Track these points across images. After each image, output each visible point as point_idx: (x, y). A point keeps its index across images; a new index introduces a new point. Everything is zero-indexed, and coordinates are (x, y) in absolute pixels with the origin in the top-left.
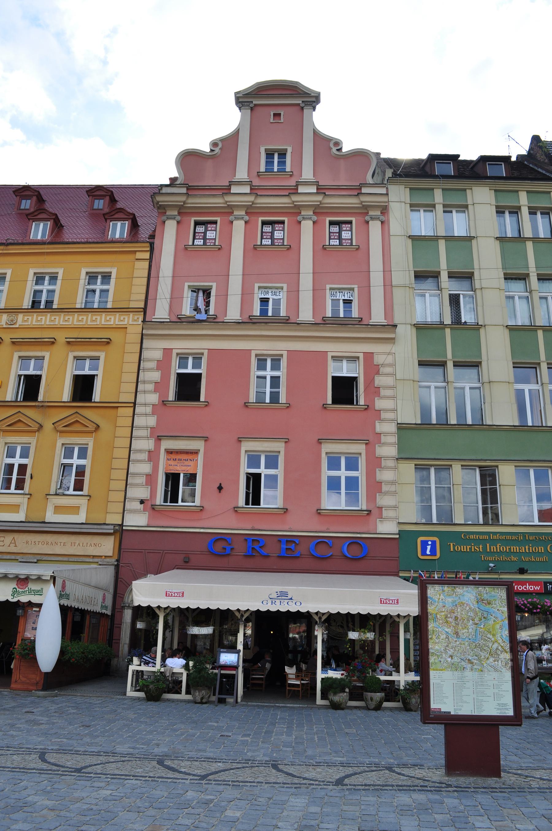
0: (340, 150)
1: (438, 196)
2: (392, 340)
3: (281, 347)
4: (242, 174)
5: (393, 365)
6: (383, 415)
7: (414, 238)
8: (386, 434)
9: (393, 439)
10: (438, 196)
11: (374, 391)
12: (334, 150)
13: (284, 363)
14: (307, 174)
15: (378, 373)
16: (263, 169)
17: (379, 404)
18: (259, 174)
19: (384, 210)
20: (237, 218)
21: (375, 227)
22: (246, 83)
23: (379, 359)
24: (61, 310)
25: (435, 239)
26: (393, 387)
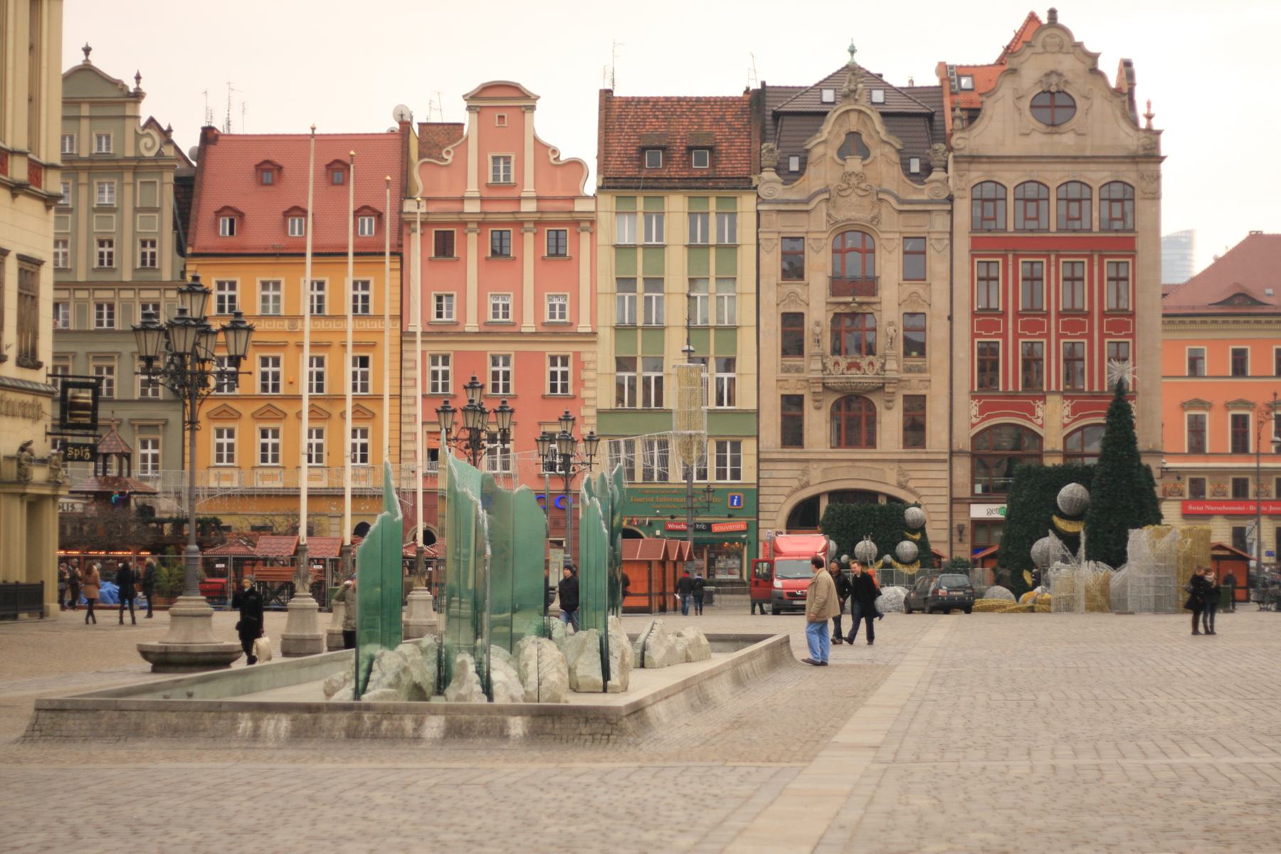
0: (557, 159)
1: (640, 203)
2: (594, 342)
3: (509, 349)
4: (473, 189)
5: (594, 362)
6: (587, 402)
7: (617, 247)
8: (588, 417)
9: (594, 421)
10: (640, 203)
11: (580, 383)
12: (552, 157)
13: (512, 361)
14: (529, 189)
15: (584, 369)
16: (490, 181)
17: (585, 394)
18: (487, 185)
19: (592, 222)
20: (471, 231)
21: (585, 238)
22: (472, 86)
23: (586, 357)
24: (331, 317)
25: (634, 247)
26: (594, 380)
